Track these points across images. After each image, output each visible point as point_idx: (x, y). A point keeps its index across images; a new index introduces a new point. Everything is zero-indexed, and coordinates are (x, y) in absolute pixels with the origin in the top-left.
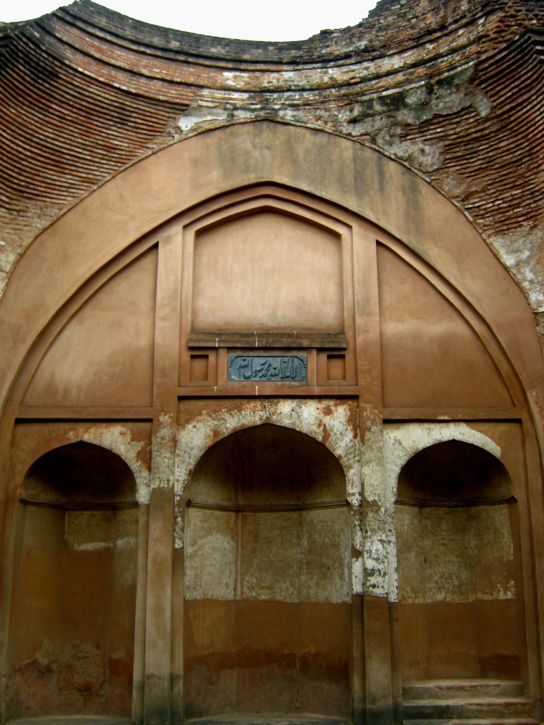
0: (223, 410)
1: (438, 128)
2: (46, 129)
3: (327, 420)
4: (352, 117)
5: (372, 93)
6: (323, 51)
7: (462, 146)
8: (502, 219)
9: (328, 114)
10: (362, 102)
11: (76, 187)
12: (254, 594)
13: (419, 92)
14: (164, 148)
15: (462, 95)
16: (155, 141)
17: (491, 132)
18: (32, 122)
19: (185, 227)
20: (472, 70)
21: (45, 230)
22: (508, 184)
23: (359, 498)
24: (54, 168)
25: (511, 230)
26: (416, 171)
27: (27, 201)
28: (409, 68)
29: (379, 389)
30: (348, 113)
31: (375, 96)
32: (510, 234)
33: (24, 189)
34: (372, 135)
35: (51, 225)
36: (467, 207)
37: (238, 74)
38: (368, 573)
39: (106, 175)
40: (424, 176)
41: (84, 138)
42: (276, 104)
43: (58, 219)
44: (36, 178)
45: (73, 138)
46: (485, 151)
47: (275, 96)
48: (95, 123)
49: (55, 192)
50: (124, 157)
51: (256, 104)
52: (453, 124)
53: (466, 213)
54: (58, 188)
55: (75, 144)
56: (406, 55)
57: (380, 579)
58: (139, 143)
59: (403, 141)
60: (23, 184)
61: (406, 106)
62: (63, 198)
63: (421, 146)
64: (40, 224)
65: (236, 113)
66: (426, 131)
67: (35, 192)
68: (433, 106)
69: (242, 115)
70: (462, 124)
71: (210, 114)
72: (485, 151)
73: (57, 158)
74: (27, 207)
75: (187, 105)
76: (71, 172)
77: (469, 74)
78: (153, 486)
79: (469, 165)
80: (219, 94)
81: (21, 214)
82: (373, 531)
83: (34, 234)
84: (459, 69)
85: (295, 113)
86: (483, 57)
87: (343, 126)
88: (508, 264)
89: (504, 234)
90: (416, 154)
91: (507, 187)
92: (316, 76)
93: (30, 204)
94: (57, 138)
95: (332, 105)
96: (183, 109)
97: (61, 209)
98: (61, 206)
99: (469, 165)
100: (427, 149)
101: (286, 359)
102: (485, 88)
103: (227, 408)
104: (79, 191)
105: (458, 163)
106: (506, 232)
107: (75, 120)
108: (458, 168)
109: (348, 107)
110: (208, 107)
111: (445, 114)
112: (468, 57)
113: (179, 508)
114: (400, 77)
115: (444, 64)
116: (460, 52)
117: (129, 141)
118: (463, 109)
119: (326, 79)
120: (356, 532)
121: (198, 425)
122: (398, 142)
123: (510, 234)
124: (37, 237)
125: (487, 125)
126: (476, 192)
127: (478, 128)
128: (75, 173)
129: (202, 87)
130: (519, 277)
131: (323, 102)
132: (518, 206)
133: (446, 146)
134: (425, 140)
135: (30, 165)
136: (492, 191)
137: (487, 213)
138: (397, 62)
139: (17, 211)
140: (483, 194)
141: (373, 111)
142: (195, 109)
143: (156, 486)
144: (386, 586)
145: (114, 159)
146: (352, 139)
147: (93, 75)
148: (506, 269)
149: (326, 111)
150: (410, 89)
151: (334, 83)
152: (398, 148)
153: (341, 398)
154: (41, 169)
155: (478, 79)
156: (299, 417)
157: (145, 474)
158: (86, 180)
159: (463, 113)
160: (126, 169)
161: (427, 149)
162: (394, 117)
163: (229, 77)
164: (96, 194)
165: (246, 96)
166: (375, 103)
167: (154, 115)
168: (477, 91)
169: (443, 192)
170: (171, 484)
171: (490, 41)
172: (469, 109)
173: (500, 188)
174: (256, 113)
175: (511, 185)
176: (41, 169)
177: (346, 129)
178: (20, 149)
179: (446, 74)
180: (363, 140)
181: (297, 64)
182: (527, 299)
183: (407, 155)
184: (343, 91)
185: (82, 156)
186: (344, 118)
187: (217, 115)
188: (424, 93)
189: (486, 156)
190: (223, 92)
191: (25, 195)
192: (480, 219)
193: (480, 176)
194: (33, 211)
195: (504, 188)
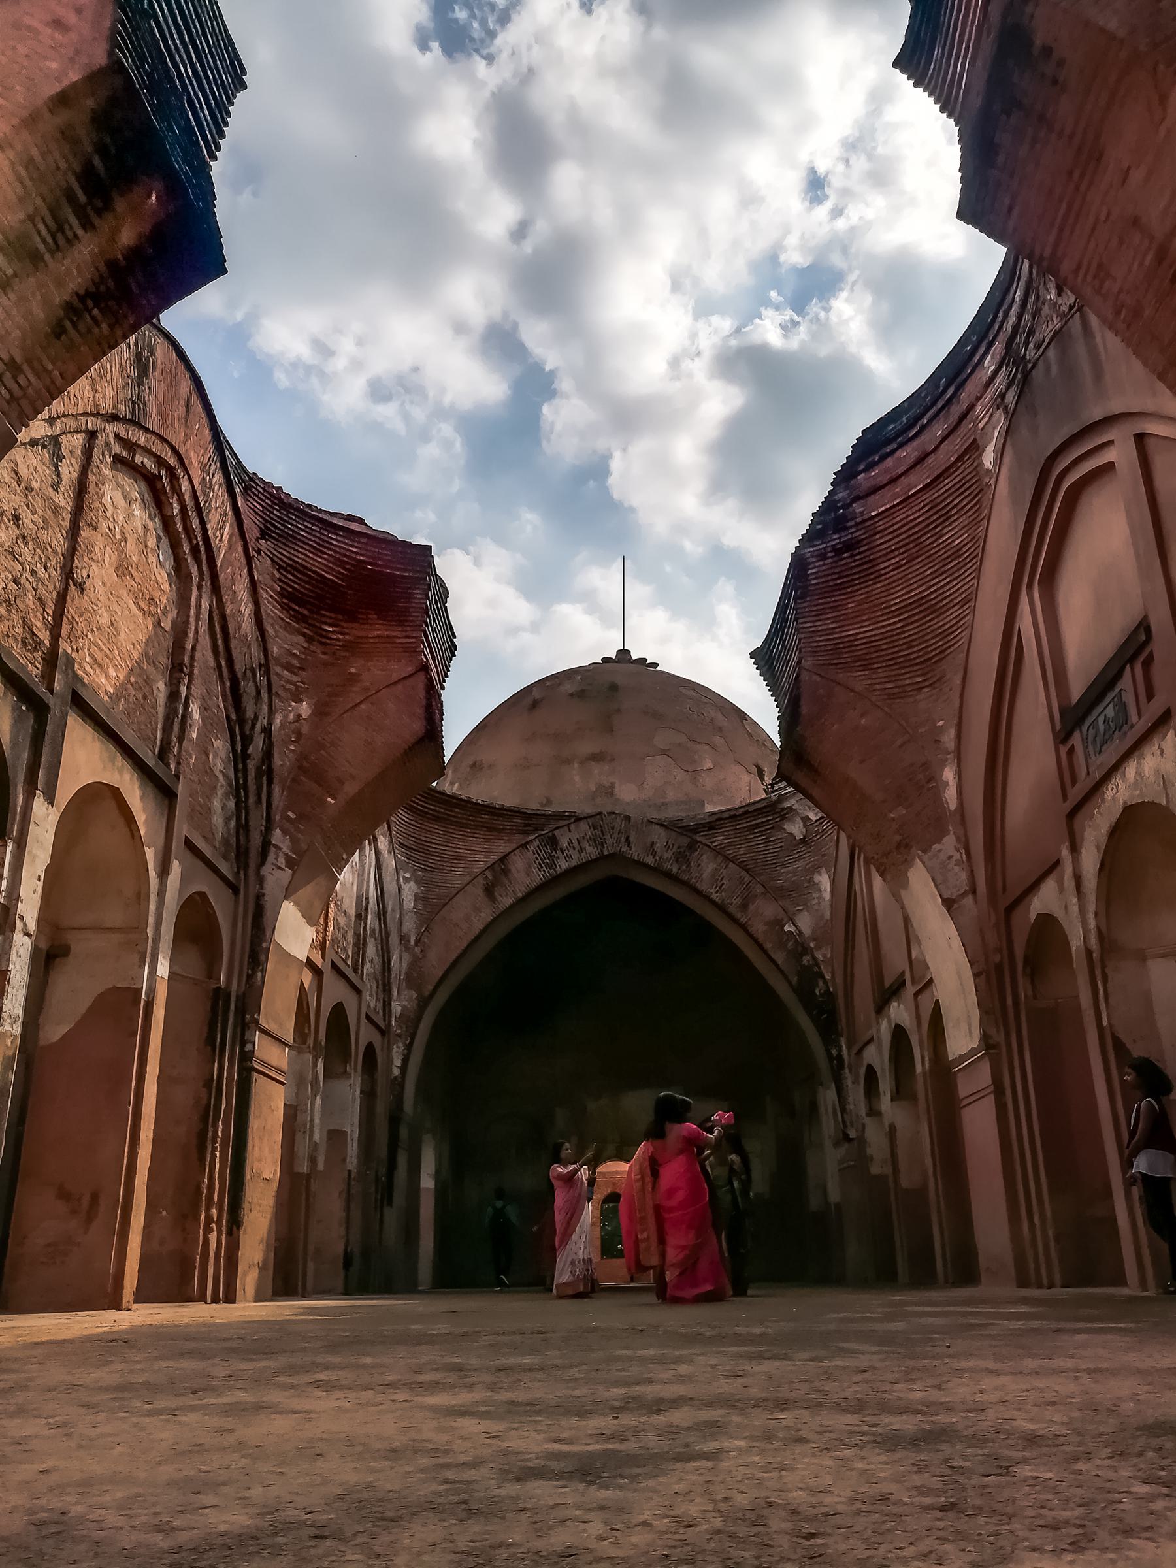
44: (927, 638)
48: (928, 542)
71: (994, 428)
75: (975, 440)
96: (975, 448)
110: (987, 422)
158: (966, 601)
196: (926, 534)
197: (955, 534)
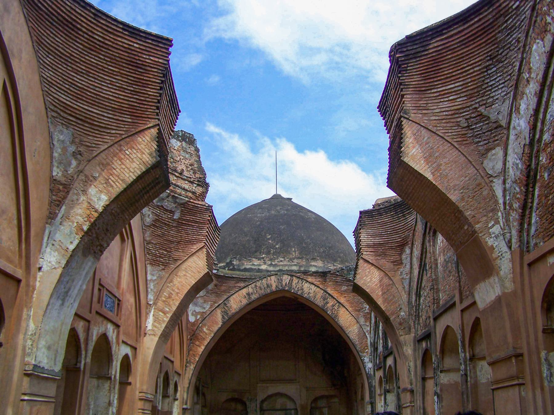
70: (166, 215)
77: (183, 201)
100: (151, 215)
112: (187, 196)
126: (153, 243)
132: (162, 258)
148: (146, 280)
172: (172, 212)
182: (147, 296)
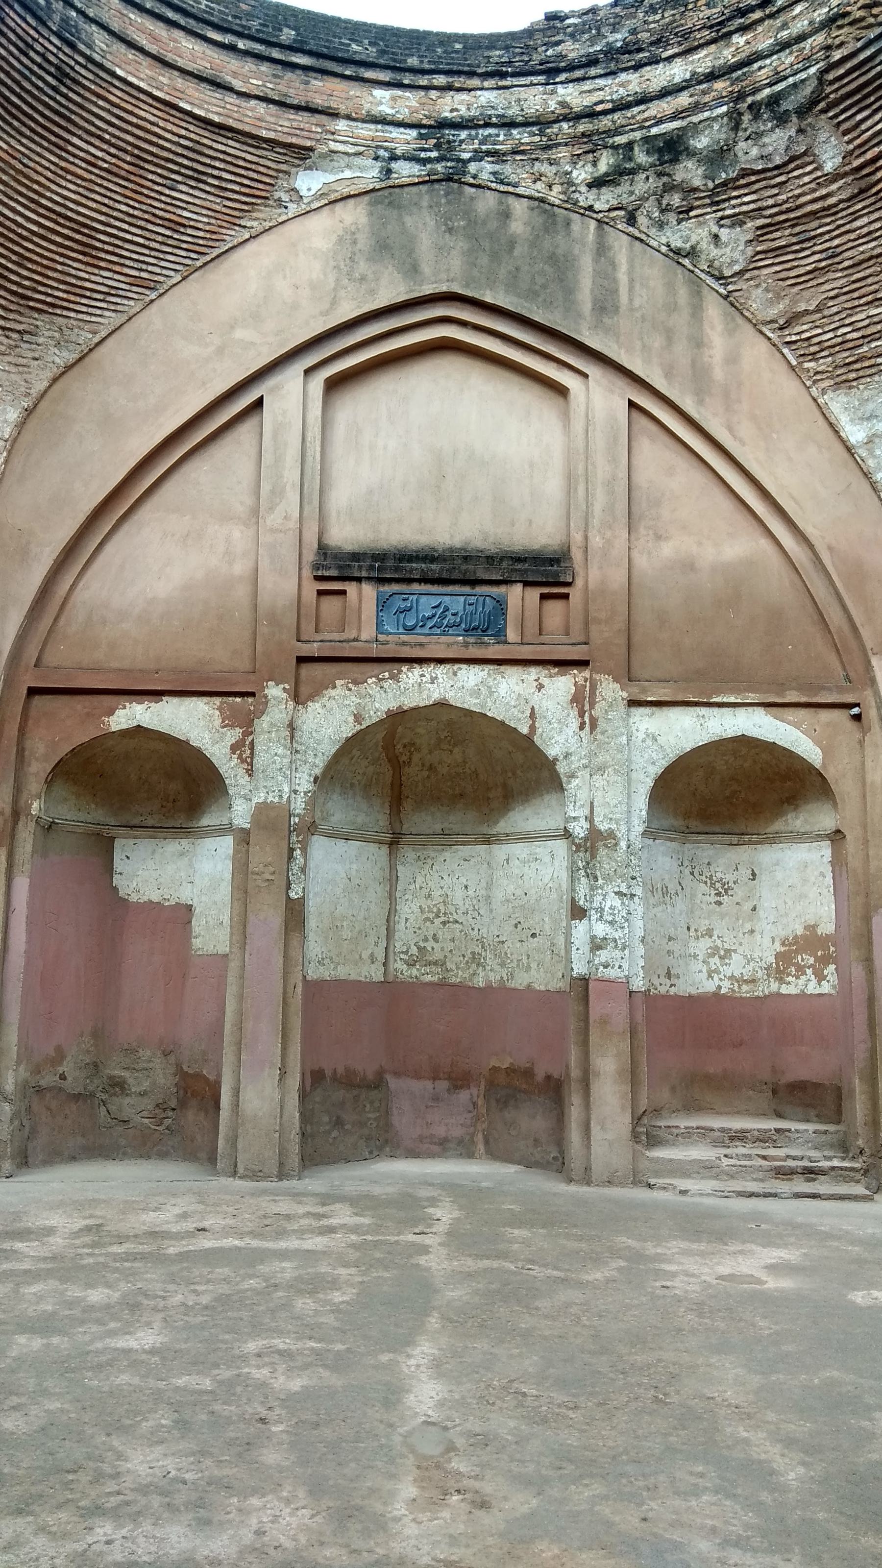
0: (370, 681)
1: (746, 195)
2: (64, 183)
3: (536, 699)
4: (596, 175)
5: (632, 130)
6: (549, 53)
7: (785, 229)
8: (847, 361)
9: (554, 169)
10: (615, 147)
11: (121, 293)
12: (415, 972)
13: (716, 127)
14: (271, 228)
15: (793, 132)
16: (255, 215)
17: (841, 201)
18: (39, 169)
19: (308, 372)
20: (814, 83)
21: (69, 368)
22: (864, 296)
23: (587, 825)
24: (81, 257)
25: (863, 380)
26: (703, 276)
27: (36, 315)
28: (700, 83)
29: (624, 649)
30: (589, 168)
31: (638, 135)
32: (861, 387)
33: (29, 293)
34: (630, 208)
35: (80, 359)
36: (788, 339)
37: (399, 93)
38: (597, 945)
39: (172, 273)
40: (715, 285)
41: (131, 203)
42: (464, 151)
43: (91, 350)
44: (50, 273)
45: (111, 203)
46: (827, 237)
47: (464, 134)
48: (150, 176)
49: (84, 301)
50: (201, 242)
51: (430, 150)
52: (773, 186)
53: (786, 351)
54: (88, 294)
55: (115, 214)
56: (696, 57)
57: (618, 954)
58: (227, 218)
59: (682, 220)
60: (26, 283)
61: (691, 153)
62: (99, 312)
63: (715, 229)
64: (62, 357)
65: (394, 165)
66: (724, 201)
67: (49, 300)
68: (740, 154)
69: (405, 171)
71: (348, 166)
72: (827, 237)
73: (84, 239)
74: (37, 326)
75: (311, 149)
76: (110, 266)
77: (808, 90)
78: (255, 800)
79: (795, 263)
80: (367, 131)
81: (26, 337)
82: (608, 879)
83: (49, 374)
84: (791, 80)
85: (497, 167)
86: (837, 55)
87: (580, 192)
88: (853, 440)
89: (850, 388)
90: (704, 245)
91: (862, 301)
92: (534, 98)
93: (41, 321)
94: (84, 201)
95: (563, 153)
96: (301, 154)
97: (95, 333)
98: (94, 327)
99: (795, 263)
100: (724, 233)
101: (472, 599)
102: (836, 116)
103: (377, 677)
104: (125, 302)
105: (777, 260)
106: (855, 384)
107: (115, 169)
108: (778, 268)
109: (590, 156)
111: (760, 167)
113: (297, 836)
114: (684, 100)
115: (763, 71)
116: (795, 48)
117: (210, 213)
118: (792, 159)
119: (553, 105)
120: (579, 879)
121: (328, 704)
122: (675, 223)
123: (861, 387)
124: (55, 380)
125: (834, 187)
126: (807, 312)
127: (817, 194)
128: (117, 268)
129: (334, 115)
130: (871, 463)
131: (548, 148)
133: (758, 228)
134: (722, 218)
135: (38, 250)
136: (835, 309)
137: (822, 350)
138: (678, 71)
139: (19, 332)
140: (819, 315)
141: (632, 165)
142: (323, 156)
143: (261, 801)
144: (625, 966)
145: (184, 246)
146: (595, 216)
147: (142, 85)
148: (849, 449)
149: (551, 164)
150: (701, 122)
151: (567, 111)
152: (674, 234)
153: (563, 664)
154: (57, 258)
155: (823, 99)
156: (491, 693)
157: (244, 780)
159: (792, 165)
160: (205, 264)
161: (724, 233)
162: (669, 175)
163: (382, 101)
164: (154, 307)
165: (414, 133)
166: (636, 149)
167: (253, 167)
168: (822, 123)
169: (747, 314)
170: (285, 797)
171: (851, 24)
173: (849, 305)
174: (429, 166)
175: (870, 298)
176: (57, 258)
177: (586, 197)
178: (19, 219)
179: (767, 91)
180: (613, 219)
181: (503, 75)
183: (688, 246)
184: (581, 128)
185: (128, 237)
186: (583, 176)
187: (361, 169)
188: (724, 129)
189: (827, 245)
190: (372, 126)
191: (31, 304)
192: (810, 361)
193: (814, 282)
194: (47, 334)
195: (856, 303)
196: (156, 165)
197: (194, 205)
